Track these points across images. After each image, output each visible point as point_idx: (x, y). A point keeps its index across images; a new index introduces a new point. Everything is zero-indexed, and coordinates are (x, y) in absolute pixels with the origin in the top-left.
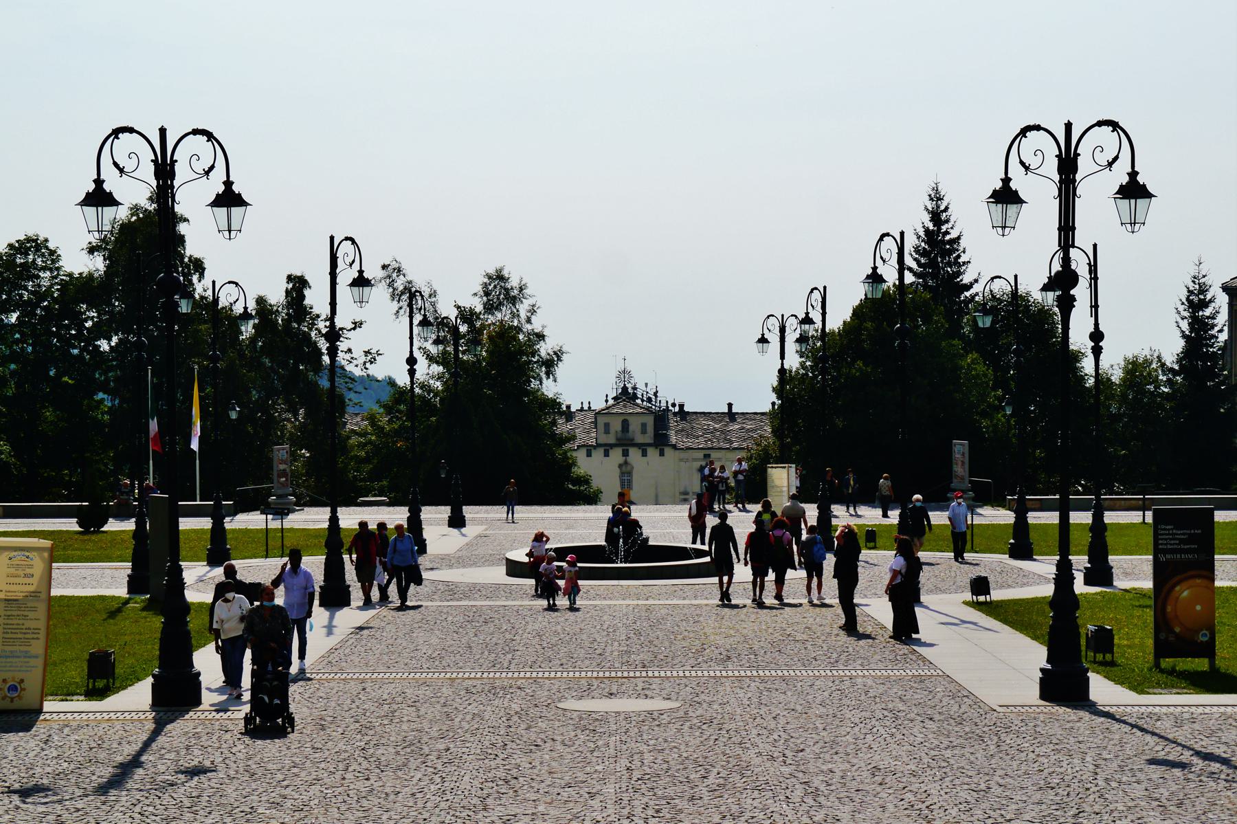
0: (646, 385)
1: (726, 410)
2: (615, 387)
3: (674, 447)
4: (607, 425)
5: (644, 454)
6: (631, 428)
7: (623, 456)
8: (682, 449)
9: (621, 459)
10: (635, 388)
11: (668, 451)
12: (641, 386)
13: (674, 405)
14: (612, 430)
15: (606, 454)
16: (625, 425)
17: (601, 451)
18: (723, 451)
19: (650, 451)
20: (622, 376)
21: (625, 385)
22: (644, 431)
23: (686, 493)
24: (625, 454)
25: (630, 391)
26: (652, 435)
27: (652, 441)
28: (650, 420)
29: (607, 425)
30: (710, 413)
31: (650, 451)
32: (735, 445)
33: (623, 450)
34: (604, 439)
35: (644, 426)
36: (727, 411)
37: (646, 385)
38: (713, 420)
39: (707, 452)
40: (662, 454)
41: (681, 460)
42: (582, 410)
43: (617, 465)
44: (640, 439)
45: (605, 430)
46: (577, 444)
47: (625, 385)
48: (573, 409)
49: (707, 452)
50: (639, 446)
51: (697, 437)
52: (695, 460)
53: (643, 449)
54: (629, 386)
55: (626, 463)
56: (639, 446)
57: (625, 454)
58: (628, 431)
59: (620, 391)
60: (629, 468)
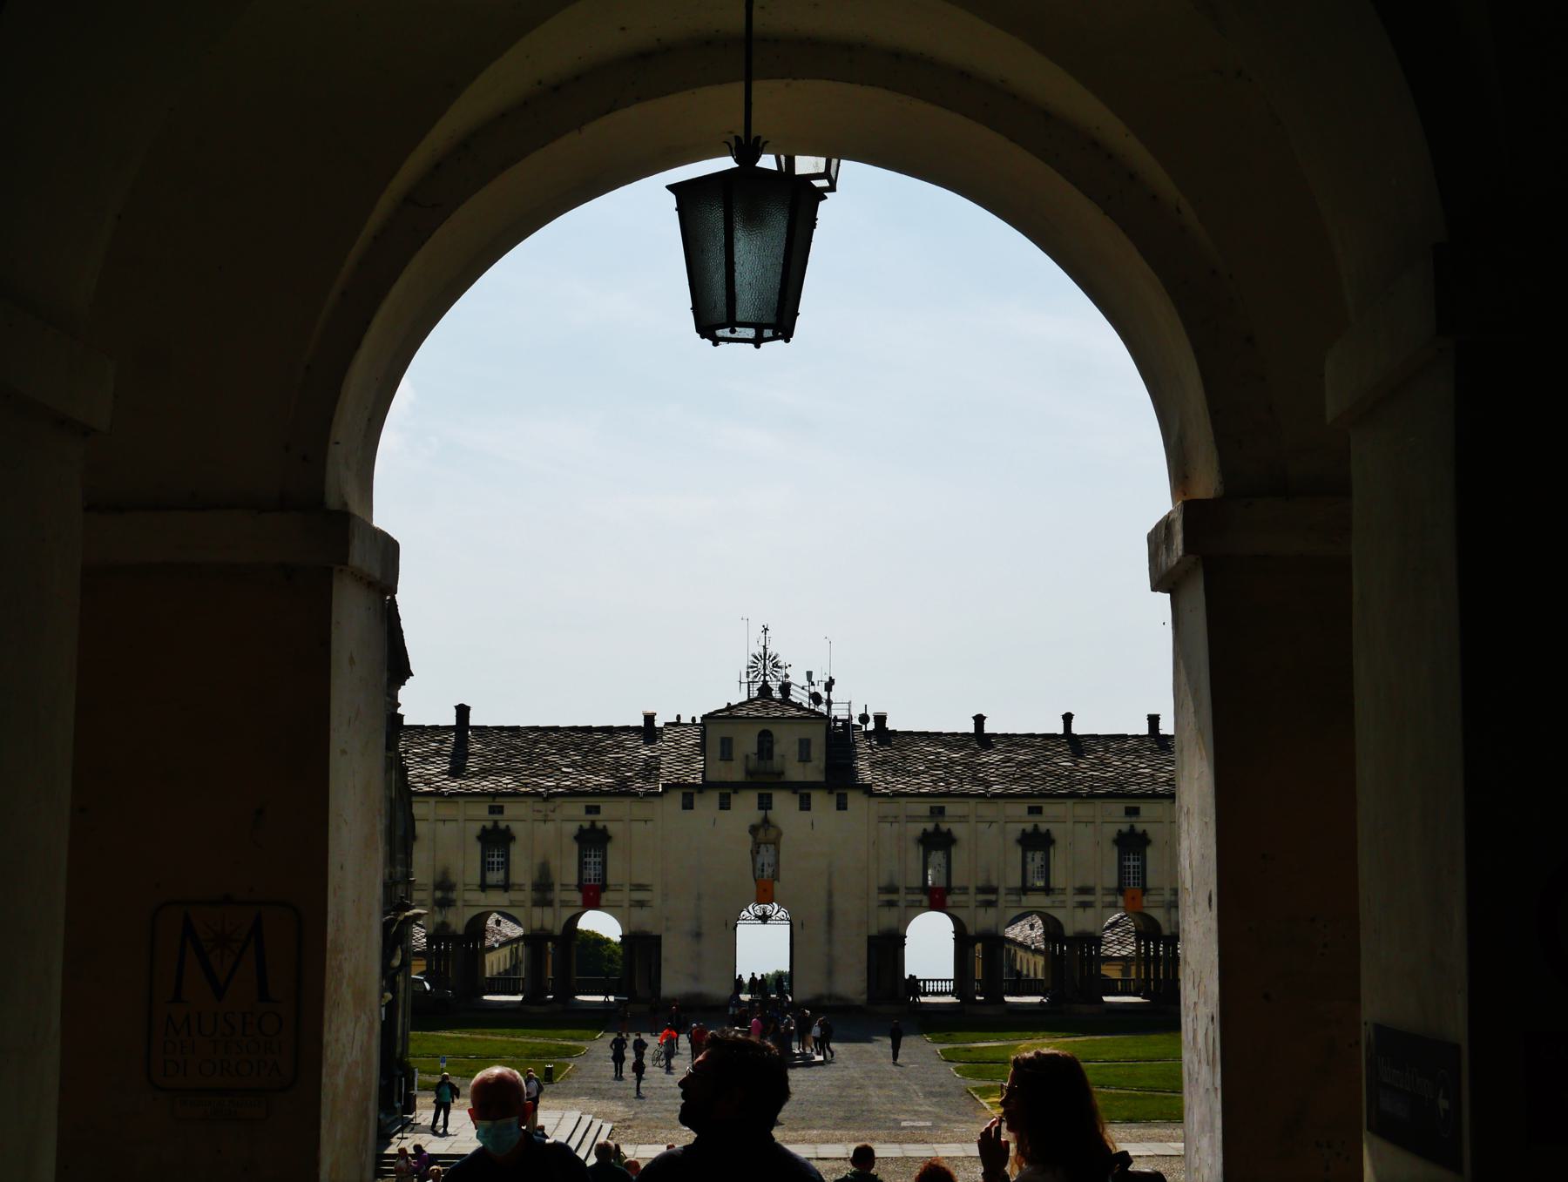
0: (809, 674)
1: (972, 730)
2: (744, 679)
3: (868, 790)
5: (805, 805)
6: (777, 750)
7: (760, 808)
9: (756, 816)
10: (785, 688)
12: (797, 678)
13: (864, 718)
14: (738, 753)
15: (725, 805)
16: (766, 740)
17: (713, 798)
18: (972, 802)
19: (819, 799)
20: (760, 665)
21: (765, 682)
22: (804, 756)
23: (891, 889)
24: (765, 803)
25: (777, 695)
26: (822, 765)
27: (821, 778)
28: (817, 735)
29: (727, 743)
31: (819, 799)
32: (996, 788)
33: (760, 796)
34: (721, 772)
35: (805, 745)
36: (972, 730)
37: (809, 674)
38: (946, 745)
39: (938, 802)
40: (842, 805)
41: (883, 819)
42: (677, 724)
43: (747, 829)
44: (795, 772)
45: (723, 753)
46: (662, 781)
47: (765, 682)
48: (659, 723)
49: (938, 802)
50: (794, 787)
51: (917, 774)
52: (912, 818)
53: (803, 793)
54: (774, 685)
56: (794, 787)
57: (765, 803)
58: (771, 757)
60: (772, 833)
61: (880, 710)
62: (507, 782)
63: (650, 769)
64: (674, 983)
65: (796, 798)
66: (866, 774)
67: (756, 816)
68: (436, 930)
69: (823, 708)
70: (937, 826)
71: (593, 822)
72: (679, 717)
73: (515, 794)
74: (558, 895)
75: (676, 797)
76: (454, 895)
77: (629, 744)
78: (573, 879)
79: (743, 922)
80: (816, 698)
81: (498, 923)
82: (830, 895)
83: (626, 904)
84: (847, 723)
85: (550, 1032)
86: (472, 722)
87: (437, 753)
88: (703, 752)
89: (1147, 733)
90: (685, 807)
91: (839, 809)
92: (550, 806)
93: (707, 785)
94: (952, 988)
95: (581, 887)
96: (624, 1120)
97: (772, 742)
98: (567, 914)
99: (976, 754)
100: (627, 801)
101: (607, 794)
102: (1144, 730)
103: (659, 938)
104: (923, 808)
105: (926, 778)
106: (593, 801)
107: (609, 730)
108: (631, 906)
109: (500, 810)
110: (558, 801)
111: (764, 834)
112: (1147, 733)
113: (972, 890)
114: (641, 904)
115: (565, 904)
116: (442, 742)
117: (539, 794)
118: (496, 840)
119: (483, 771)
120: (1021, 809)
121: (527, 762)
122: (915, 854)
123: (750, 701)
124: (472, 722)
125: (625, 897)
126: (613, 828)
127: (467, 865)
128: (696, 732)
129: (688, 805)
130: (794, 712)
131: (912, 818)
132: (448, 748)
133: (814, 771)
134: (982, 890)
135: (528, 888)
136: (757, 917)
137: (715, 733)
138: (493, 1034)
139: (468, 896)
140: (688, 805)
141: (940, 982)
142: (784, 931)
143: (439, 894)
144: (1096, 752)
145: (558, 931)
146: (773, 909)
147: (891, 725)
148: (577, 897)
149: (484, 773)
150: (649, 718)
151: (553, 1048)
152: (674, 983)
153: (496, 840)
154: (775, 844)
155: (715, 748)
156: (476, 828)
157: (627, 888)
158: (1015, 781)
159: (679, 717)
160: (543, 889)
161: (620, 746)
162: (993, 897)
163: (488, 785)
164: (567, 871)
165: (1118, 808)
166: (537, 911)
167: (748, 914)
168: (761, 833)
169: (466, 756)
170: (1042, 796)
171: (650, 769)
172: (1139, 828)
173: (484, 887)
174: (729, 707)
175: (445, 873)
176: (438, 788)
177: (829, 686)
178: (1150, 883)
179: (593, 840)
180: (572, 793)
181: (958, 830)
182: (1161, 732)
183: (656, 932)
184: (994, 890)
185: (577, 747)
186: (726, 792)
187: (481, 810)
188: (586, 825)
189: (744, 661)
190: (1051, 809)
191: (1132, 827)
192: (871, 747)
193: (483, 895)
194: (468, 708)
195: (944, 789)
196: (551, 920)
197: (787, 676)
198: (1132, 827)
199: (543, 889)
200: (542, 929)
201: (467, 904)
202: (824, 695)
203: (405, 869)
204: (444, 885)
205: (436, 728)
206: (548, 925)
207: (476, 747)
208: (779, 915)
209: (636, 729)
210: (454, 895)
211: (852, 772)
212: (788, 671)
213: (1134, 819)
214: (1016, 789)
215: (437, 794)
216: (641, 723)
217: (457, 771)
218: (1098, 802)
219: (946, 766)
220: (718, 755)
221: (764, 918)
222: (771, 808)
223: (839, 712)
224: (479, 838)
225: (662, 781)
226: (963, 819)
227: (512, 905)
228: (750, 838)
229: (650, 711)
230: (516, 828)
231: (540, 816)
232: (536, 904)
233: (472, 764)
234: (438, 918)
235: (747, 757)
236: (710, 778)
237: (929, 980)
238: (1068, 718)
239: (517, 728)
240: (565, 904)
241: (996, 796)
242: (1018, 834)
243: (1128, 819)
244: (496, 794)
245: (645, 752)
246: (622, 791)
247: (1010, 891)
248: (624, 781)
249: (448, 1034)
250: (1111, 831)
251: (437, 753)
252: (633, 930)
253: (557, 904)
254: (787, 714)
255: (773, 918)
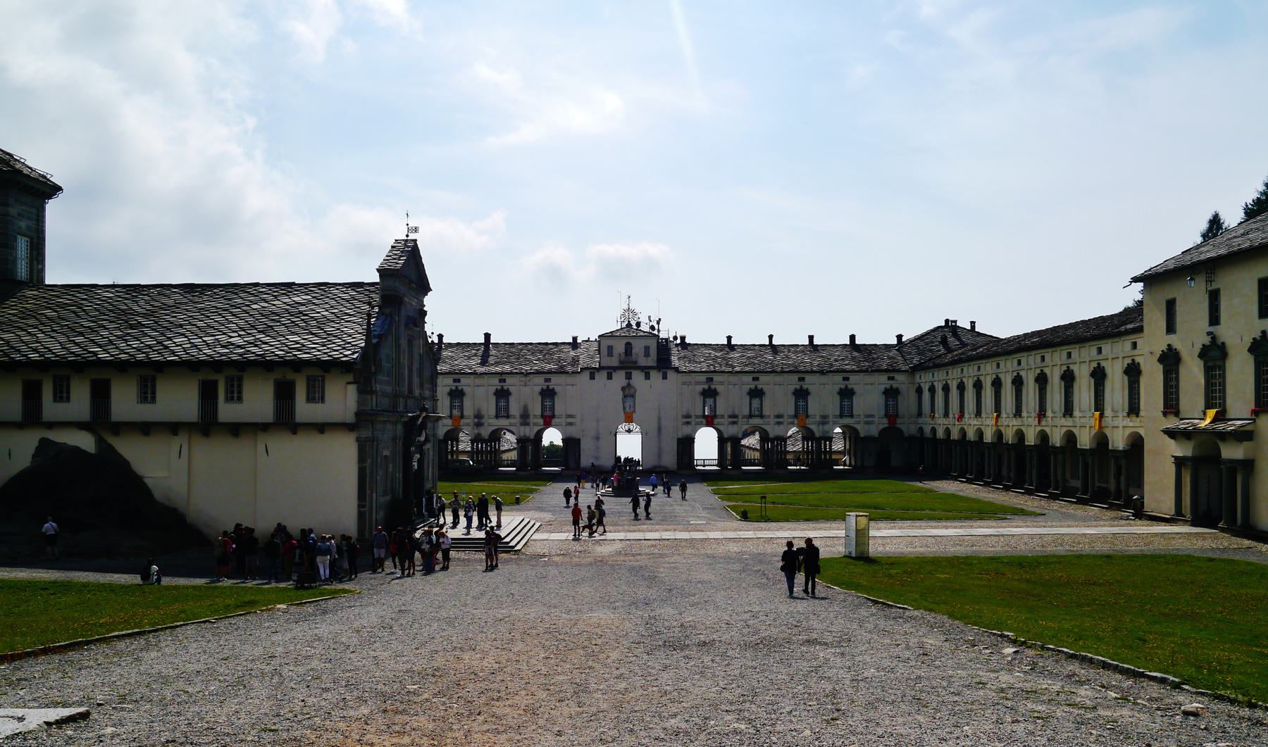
0: (649, 317)
1: (726, 343)
2: (619, 320)
3: (677, 370)
4: (610, 348)
5: (647, 377)
6: (633, 351)
8: (685, 372)
9: (624, 382)
10: (638, 324)
11: (671, 374)
12: (644, 320)
13: (675, 338)
14: (616, 352)
15: (610, 377)
16: (629, 346)
17: (604, 374)
18: (726, 375)
19: (653, 374)
20: (627, 314)
21: (629, 322)
22: (647, 354)
23: (688, 416)
24: (629, 377)
26: (655, 358)
28: (653, 344)
29: (610, 348)
30: (711, 345)
31: (653, 374)
32: (737, 369)
34: (608, 362)
35: (647, 349)
36: (726, 343)
37: (649, 317)
38: (713, 349)
39: (710, 375)
40: (665, 377)
41: (684, 383)
42: (588, 340)
44: (643, 362)
46: (580, 366)
47: (629, 322)
48: (579, 341)
49: (710, 375)
50: (642, 369)
51: (700, 363)
52: (698, 383)
53: (646, 371)
54: (633, 323)
55: (629, 384)
56: (642, 369)
57: (629, 377)
58: (631, 354)
59: (624, 325)
61: (683, 334)
62: (507, 368)
63: (575, 361)
64: (586, 461)
65: (643, 374)
66: (675, 361)
67: (624, 382)
68: (476, 437)
69: (656, 332)
70: (709, 387)
71: (548, 386)
72: (589, 338)
73: (511, 373)
74: (532, 420)
75: (587, 374)
76: (483, 421)
77: (565, 350)
78: (538, 412)
80: (652, 328)
81: (505, 433)
82: (659, 419)
83: (564, 424)
84: (667, 340)
85: (525, 483)
86: (492, 341)
87: (475, 355)
88: (599, 354)
89: (808, 344)
90: (591, 379)
91: (663, 379)
92: (528, 378)
93: (601, 368)
95: (542, 416)
96: (549, 521)
97: (631, 348)
98: (536, 429)
99: (728, 353)
100: (563, 376)
101: (555, 373)
102: (807, 342)
103: (580, 439)
104: (703, 378)
105: (704, 365)
106: (548, 376)
107: (556, 344)
108: (566, 425)
109: (504, 381)
110: (532, 376)
111: (628, 393)
112: (808, 344)
113: (726, 417)
114: (571, 424)
115: (535, 424)
116: (477, 350)
117: (522, 373)
118: (503, 394)
119: (496, 363)
120: (748, 378)
121: (517, 359)
122: (699, 400)
123: (622, 329)
124: (492, 341)
125: (563, 421)
126: (557, 389)
127: (489, 407)
128: (596, 344)
129: (592, 377)
130: (642, 334)
131: (698, 383)
132: (480, 353)
133: (651, 361)
134: (730, 417)
135: (518, 417)
136: (627, 431)
137: (605, 343)
138: (499, 484)
139: (490, 421)
140: (592, 377)
142: (639, 436)
143: (476, 420)
144: (784, 352)
145: (532, 437)
147: (687, 341)
148: (541, 421)
149: (497, 364)
150: (575, 339)
151: (524, 489)
152: (586, 461)
153: (503, 394)
154: (633, 396)
155: (604, 351)
156: (493, 389)
157: (564, 417)
158: (746, 365)
159: (589, 338)
160: (525, 417)
161: (561, 351)
162: (735, 420)
163: (498, 369)
164: (536, 409)
165: (795, 378)
166: (522, 428)
168: (627, 390)
169: (489, 356)
170: (758, 372)
171: (575, 361)
172: (805, 387)
173: (497, 417)
174: (611, 332)
175: (479, 411)
176: (475, 371)
177: (658, 323)
178: (810, 412)
179: (548, 394)
180: (538, 372)
181: (720, 388)
182: (815, 343)
183: (578, 437)
184: (736, 416)
185: (541, 352)
186: (610, 371)
187: (495, 381)
188: (545, 387)
189: (619, 312)
190: (763, 378)
191: (801, 386)
192: (678, 351)
193: (497, 420)
194: (490, 335)
195: (713, 369)
196: (529, 432)
197: (639, 318)
198: (801, 386)
199: (525, 417)
200: (525, 436)
201: (489, 425)
202: (656, 327)
203: (432, 393)
204: (479, 416)
205: (475, 344)
206: (527, 435)
207: (493, 352)
209: (569, 344)
210: (483, 421)
211: (669, 361)
212: (639, 315)
213: (802, 383)
214: (747, 369)
215: (475, 373)
216: (571, 341)
217: (484, 362)
218: (786, 375)
219: (713, 359)
220: (606, 354)
221: (629, 431)
223: (663, 335)
224: (495, 394)
225: (580, 366)
226: (722, 383)
227: (511, 425)
228: (621, 392)
229: (575, 335)
230: (512, 389)
231: (523, 383)
232: (522, 424)
233: (491, 360)
234: (476, 432)
235: (620, 355)
236: (603, 364)
238: (771, 337)
239: (513, 344)
240: (535, 424)
241: (737, 372)
242: (747, 390)
243: (799, 383)
244: (502, 373)
245: (572, 353)
246: (561, 371)
247: (744, 417)
248: (562, 367)
249: (477, 484)
250: (792, 388)
251: (475, 355)
252: (567, 436)
253: (531, 424)
254: (639, 335)
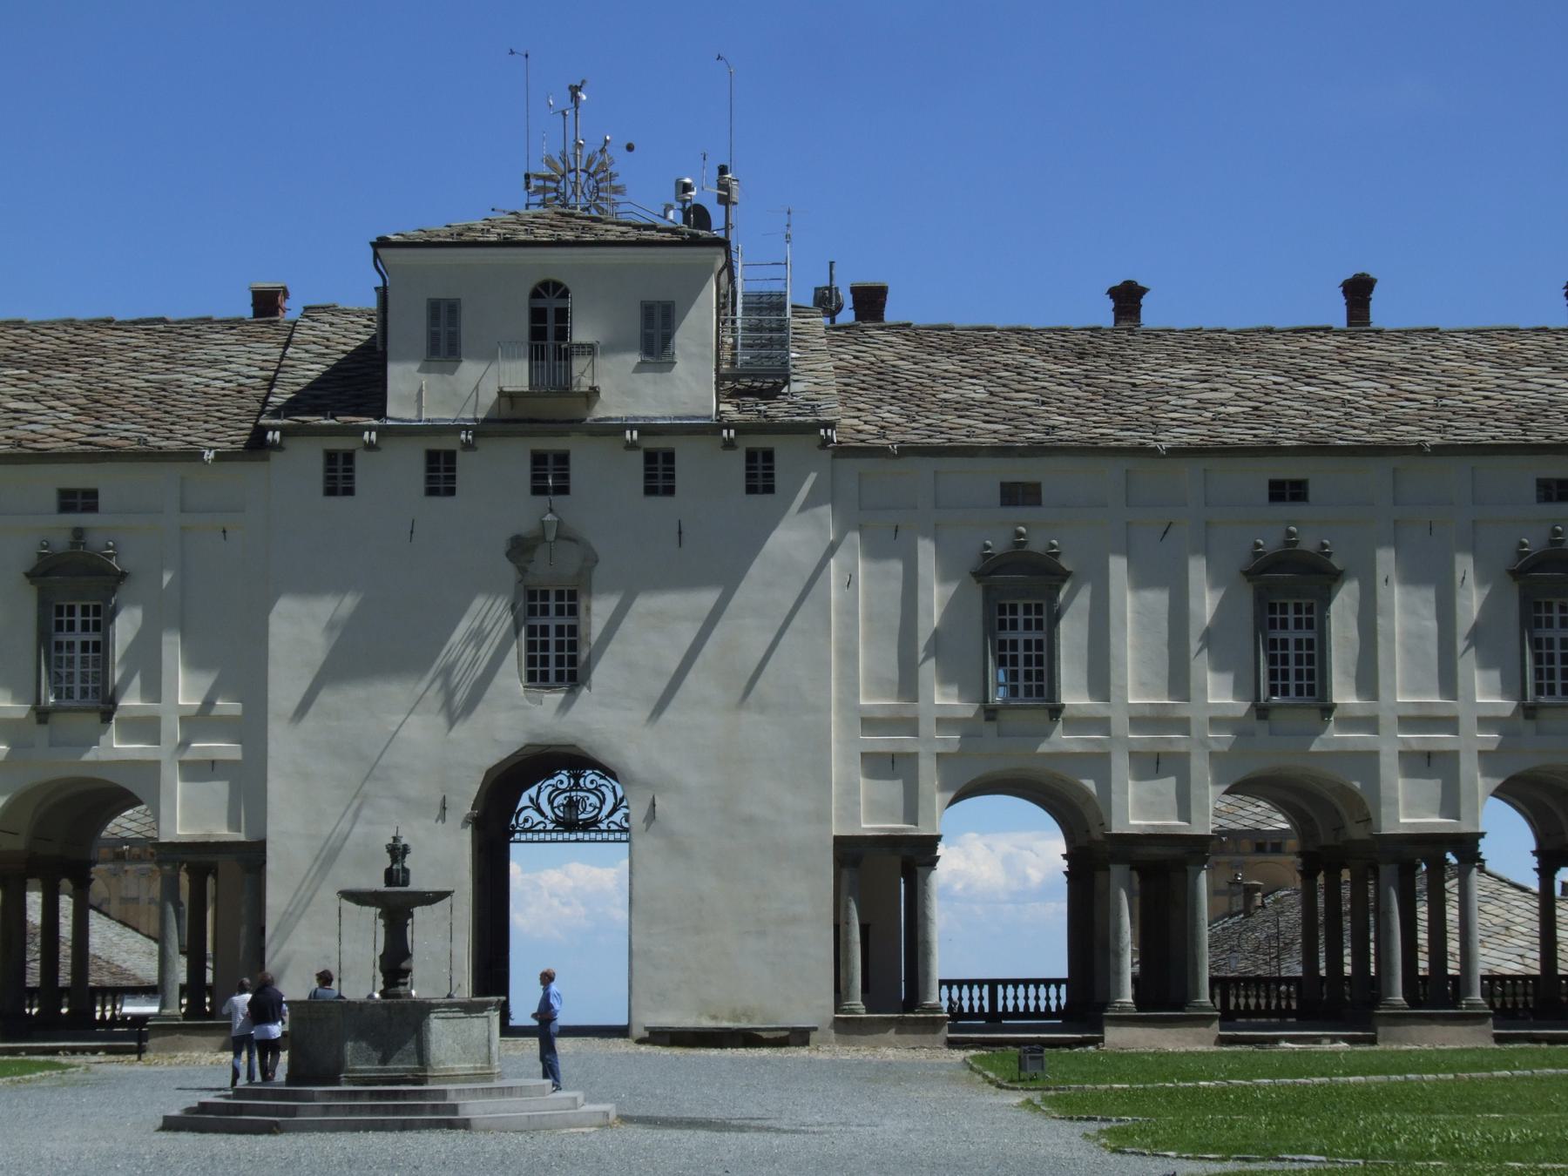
7: (538, 490)
43: (503, 546)
71: (79, 533)
79: (523, 837)
94: (1063, 1002)
141: (1032, 988)
146: (603, 802)
167: (537, 818)
208: (617, 817)
222: (563, 490)
237: (1005, 983)
255: (603, 826)
